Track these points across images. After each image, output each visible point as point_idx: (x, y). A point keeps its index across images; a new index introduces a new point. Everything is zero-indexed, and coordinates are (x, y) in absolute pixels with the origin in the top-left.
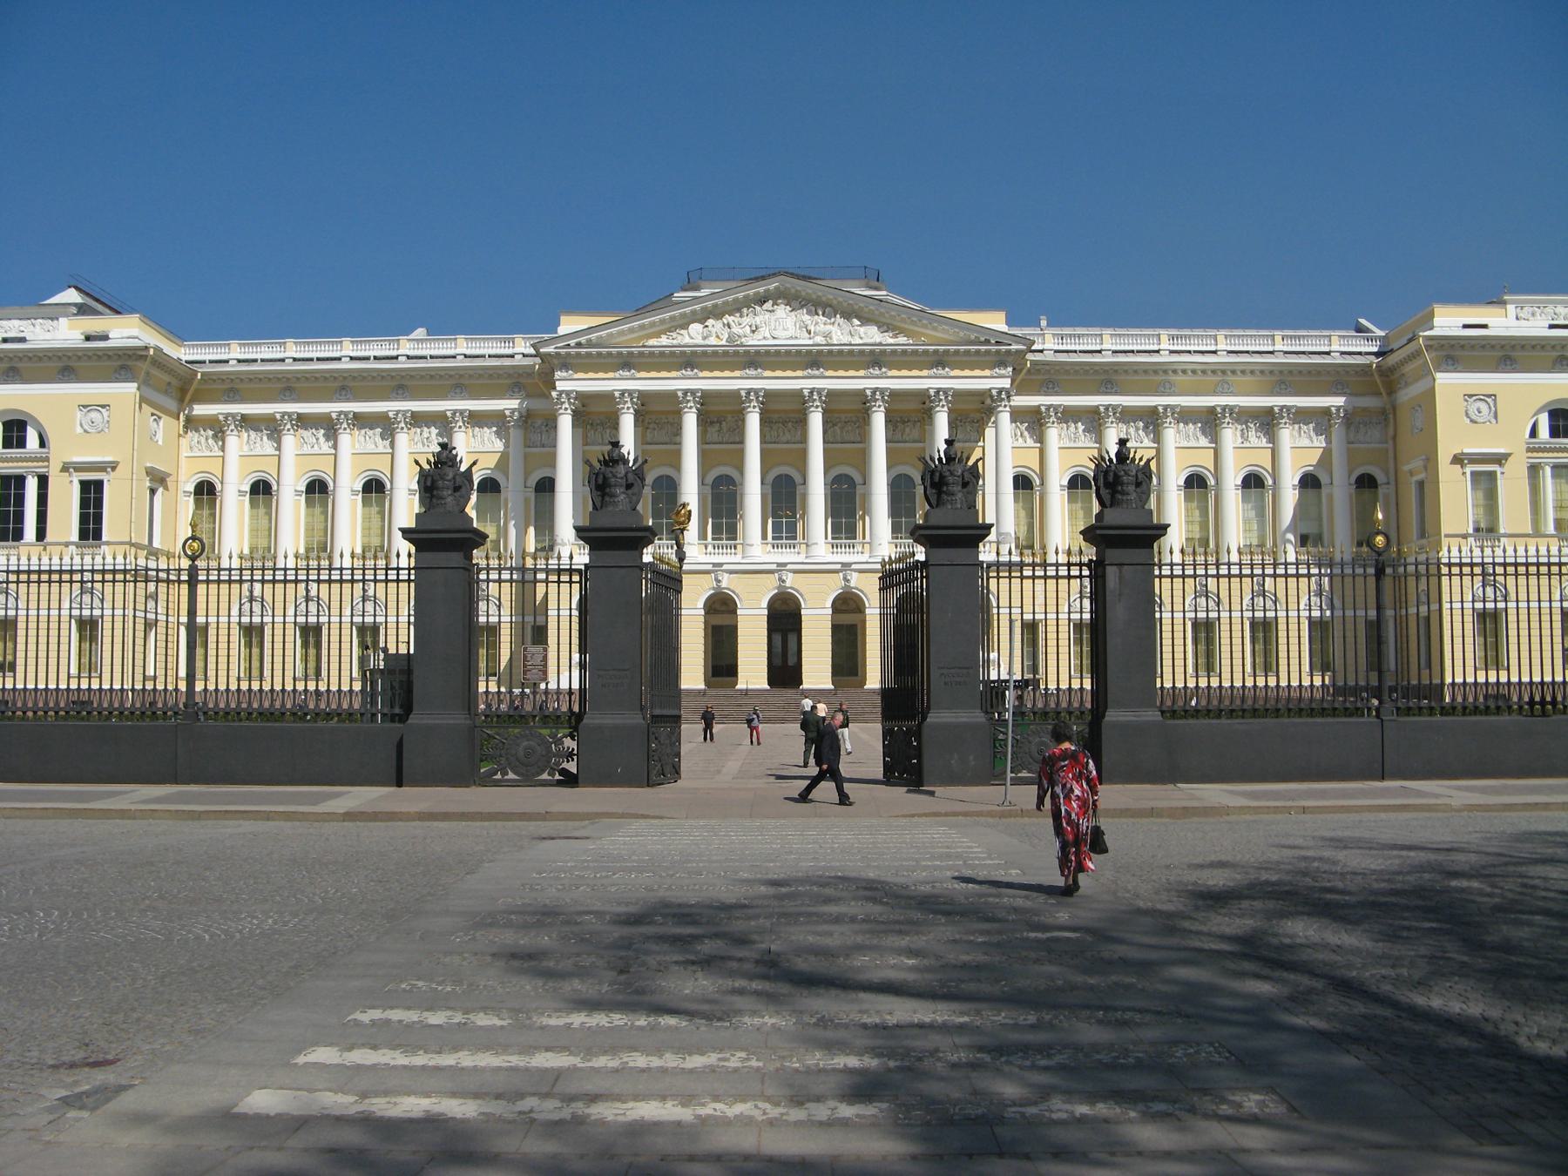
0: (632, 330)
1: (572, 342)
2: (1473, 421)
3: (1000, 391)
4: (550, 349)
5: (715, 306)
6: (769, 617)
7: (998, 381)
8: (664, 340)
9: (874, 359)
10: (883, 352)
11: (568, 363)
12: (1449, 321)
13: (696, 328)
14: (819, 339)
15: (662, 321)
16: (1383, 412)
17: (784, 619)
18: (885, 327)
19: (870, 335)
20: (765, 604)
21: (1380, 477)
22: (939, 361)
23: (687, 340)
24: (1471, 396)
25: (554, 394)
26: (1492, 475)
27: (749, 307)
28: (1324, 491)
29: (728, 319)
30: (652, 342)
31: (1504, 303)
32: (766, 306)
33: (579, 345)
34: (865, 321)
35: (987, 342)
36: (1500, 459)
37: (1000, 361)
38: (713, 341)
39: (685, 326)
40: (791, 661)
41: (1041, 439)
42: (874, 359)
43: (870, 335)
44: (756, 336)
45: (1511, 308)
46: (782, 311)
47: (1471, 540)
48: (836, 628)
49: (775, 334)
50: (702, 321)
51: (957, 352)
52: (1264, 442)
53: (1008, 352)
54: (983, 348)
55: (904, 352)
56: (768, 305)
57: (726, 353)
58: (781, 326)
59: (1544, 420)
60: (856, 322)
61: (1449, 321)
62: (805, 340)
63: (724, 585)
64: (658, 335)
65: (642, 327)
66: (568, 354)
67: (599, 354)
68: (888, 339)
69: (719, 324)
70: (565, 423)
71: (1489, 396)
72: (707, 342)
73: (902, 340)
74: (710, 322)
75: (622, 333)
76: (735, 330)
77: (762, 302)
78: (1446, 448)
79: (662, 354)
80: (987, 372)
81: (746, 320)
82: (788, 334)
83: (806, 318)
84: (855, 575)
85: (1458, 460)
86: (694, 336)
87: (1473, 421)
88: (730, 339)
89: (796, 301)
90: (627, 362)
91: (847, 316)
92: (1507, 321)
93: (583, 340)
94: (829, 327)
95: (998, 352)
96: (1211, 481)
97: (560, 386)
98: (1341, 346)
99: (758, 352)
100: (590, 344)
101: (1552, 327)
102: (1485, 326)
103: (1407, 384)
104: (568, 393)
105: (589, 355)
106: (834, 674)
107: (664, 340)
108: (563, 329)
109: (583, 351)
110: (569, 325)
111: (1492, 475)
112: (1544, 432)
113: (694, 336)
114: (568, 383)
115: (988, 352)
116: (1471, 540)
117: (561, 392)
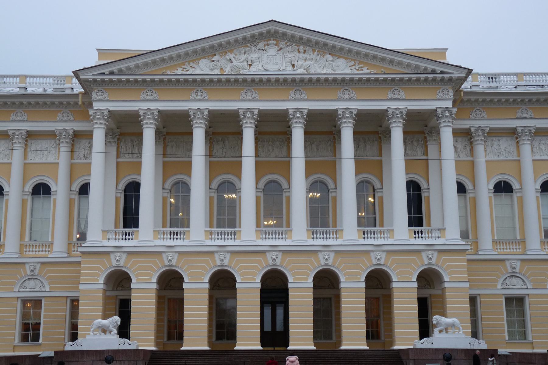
1: (106, 71)
4: (89, 76)
6: (261, 290)
7: (442, 103)
17: (274, 291)
20: (259, 280)
23: (198, 72)
25: (91, 112)
29: (230, 56)
30: (169, 73)
32: (258, 47)
33: (112, 73)
35: (433, 71)
38: (217, 72)
39: (196, 61)
40: (279, 327)
41: (472, 152)
43: (342, 68)
46: (272, 51)
48: (316, 300)
53: (450, 80)
54: (431, 76)
56: (261, 45)
60: (329, 57)
62: (289, 70)
64: (175, 67)
66: (103, 81)
82: (277, 67)
88: (233, 68)
91: (322, 53)
93: (115, 68)
94: (309, 63)
95: (442, 80)
97: (96, 106)
105: (120, 81)
106: (315, 337)
107: (180, 71)
109: (115, 78)
114: (103, 104)
115: (434, 80)
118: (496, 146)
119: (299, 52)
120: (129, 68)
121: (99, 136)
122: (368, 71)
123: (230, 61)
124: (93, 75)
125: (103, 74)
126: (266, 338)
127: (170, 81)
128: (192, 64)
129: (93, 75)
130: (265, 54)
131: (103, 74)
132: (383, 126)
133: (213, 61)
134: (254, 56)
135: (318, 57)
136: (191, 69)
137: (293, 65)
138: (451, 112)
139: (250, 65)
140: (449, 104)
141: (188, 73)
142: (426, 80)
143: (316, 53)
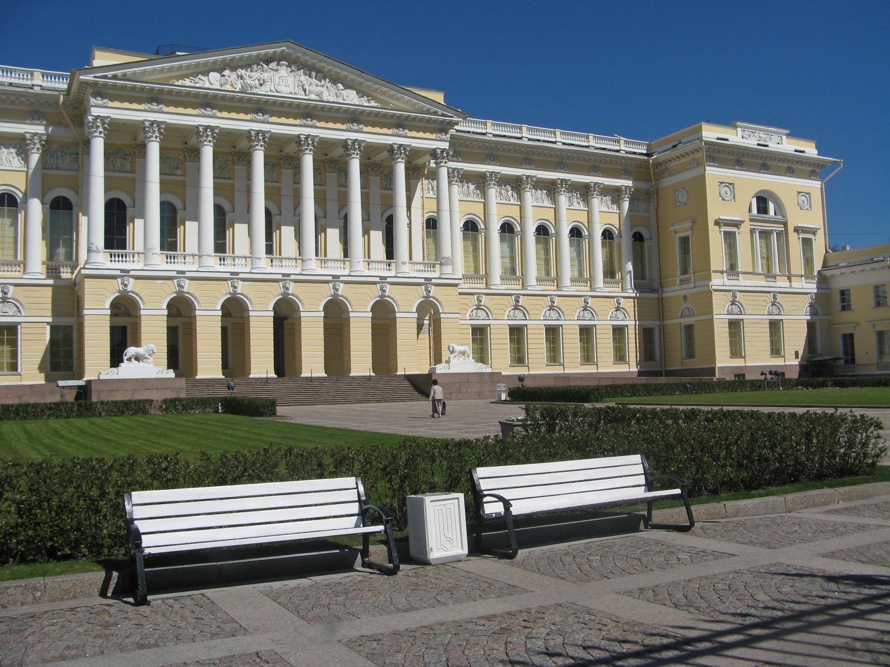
0: (162, 71)
1: (110, 74)
2: (723, 199)
3: (443, 150)
5: (232, 60)
8: (187, 82)
9: (353, 117)
10: (362, 112)
11: (101, 91)
12: (710, 133)
13: (214, 76)
14: (313, 97)
15: (188, 67)
16: (648, 193)
18: (361, 93)
19: (351, 98)
21: (646, 235)
22: (400, 123)
23: (207, 85)
24: (722, 183)
25: (90, 118)
26: (734, 233)
27: (258, 64)
28: (616, 240)
30: (180, 82)
31: (736, 127)
33: (115, 77)
34: (347, 87)
35: (435, 113)
36: (737, 224)
37: (442, 128)
39: (206, 73)
42: (353, 117)
44: (263, 88)
45: (739, 130)
46: (284, 71)
47: (725, 274)
49: (279, 88)
50: (220, 71)
51: (414, 118)
52: (582, 208)
55: (377, 114)
56: (273, 65)
57: (241, 100)
58: (282, 82)
59: (754, 201)
60: (340, 86)
61: (710, 133)
63: (239, 290)
64: (183, 77)
65: (171, 69)
66: (105, 85)
67: (133, 88)
68: (364, 101)
69: (234, 76)
70: (98, 146)
71: (730, 184)
72: (223, 88)
73: (373, 104)
74: (227, 72)
75: (153, 72)
76: (248, 81)
77: (268, 61)
78: (713, 214)
79: (188, 94)
80: (433, 136)
81: (256, 75)
82: (291, 89)
83: (304, 78)
84: (342, 285)
85: (717, 223)
86: (213, 81)
87: (723, 199)
89: (295, 64)
90: (155, 98)
91: (335, 81)
92: (739, 137)
93: (119, 73)
94: (320, 89)
95: (443, 122)
96: (552, 231)
97: (95, 112)
98: (625, 147)
99: (267, 102)
100: (124, 77)
101: (758, 145)
102: (727, 140)
103: (670, 175)
104: (103, 119)
105: (124, 87)
108: (96, 63)
110: (102, 58)
111: (734, 233)
112: (755, 210)
113: (213, 81)
115: (436, 121)
116: (725, 274)
117: (98, 117)
118: (465, 187)
119: (310, 77)
120: (135, 73)
121: (98, 146)
122: (376, 104)
123: (241, 77)
124: (95, 77)
125: (105, 77)
126: (328, 366)
127: (179, 93)
128: (200, 76)
129: (95, 77)
130: (277, 75)
131: (105, 77)
132: (372, 160)
133: (224, 76)
134: (266, 76)
135: (329, 85)
136: (201, 82)
137: (305, 90)
138: (447, 153)
139: (261, 85)
140: (446, 145)
141: (197, 85)
142: (429, 120)
143: (327, 80)
